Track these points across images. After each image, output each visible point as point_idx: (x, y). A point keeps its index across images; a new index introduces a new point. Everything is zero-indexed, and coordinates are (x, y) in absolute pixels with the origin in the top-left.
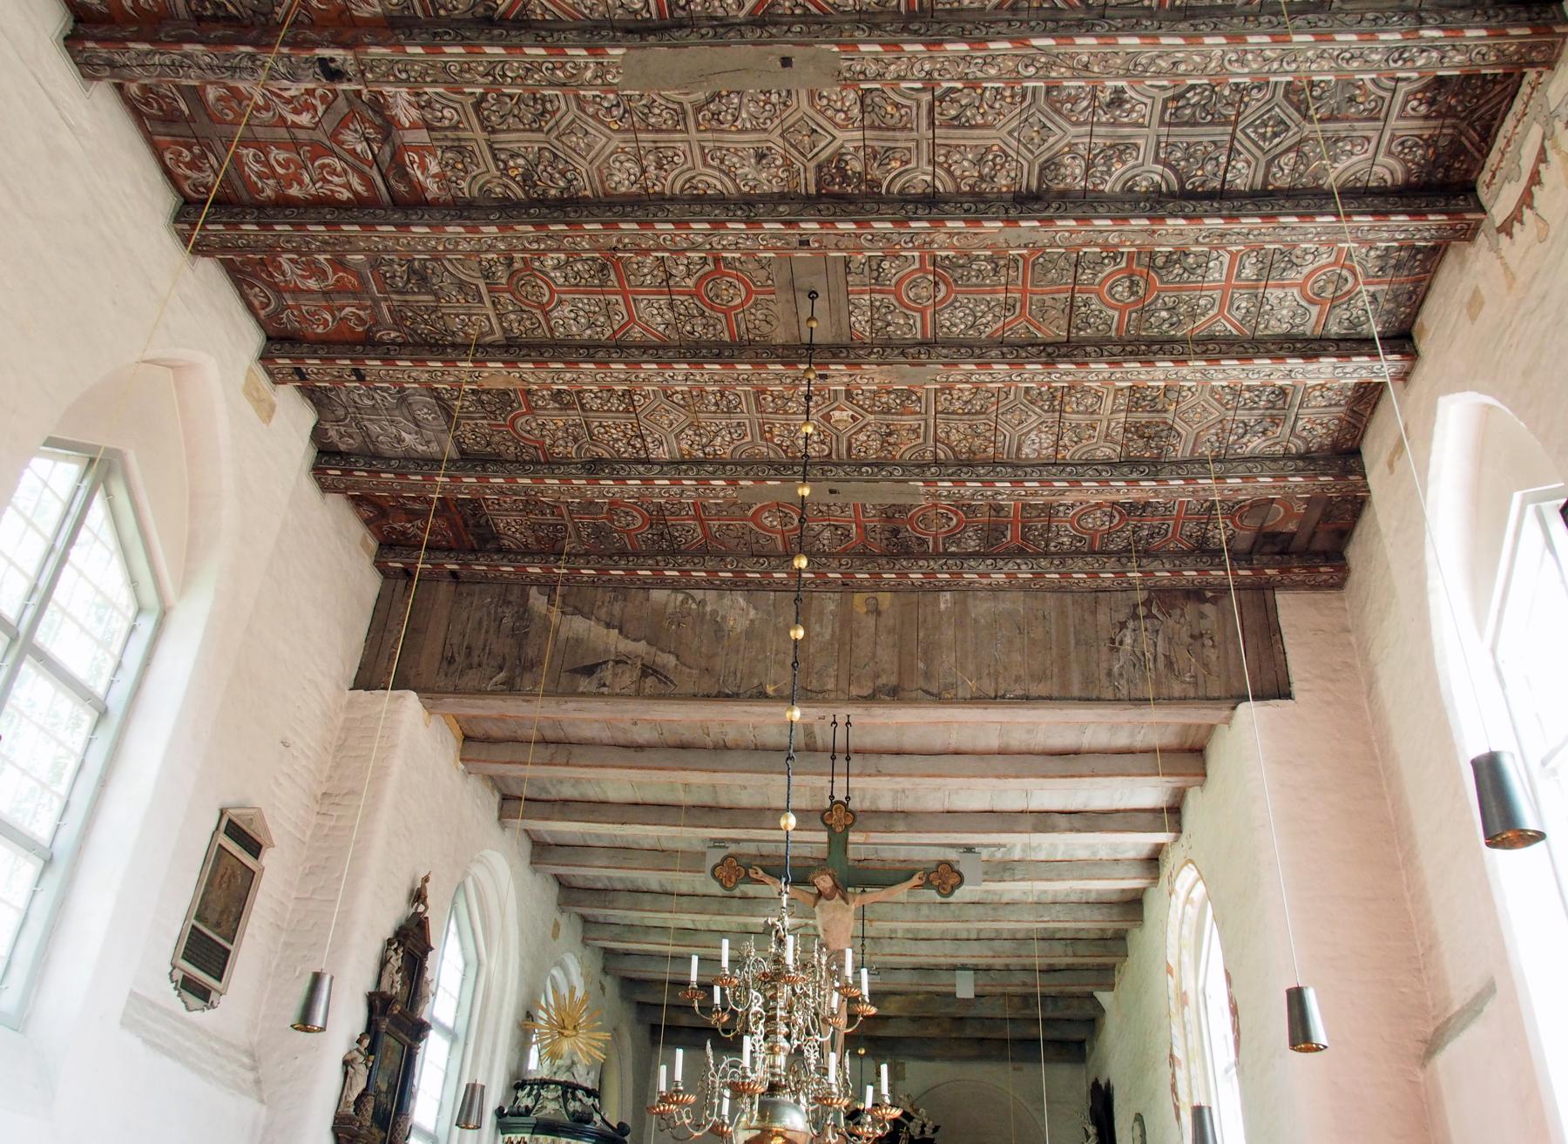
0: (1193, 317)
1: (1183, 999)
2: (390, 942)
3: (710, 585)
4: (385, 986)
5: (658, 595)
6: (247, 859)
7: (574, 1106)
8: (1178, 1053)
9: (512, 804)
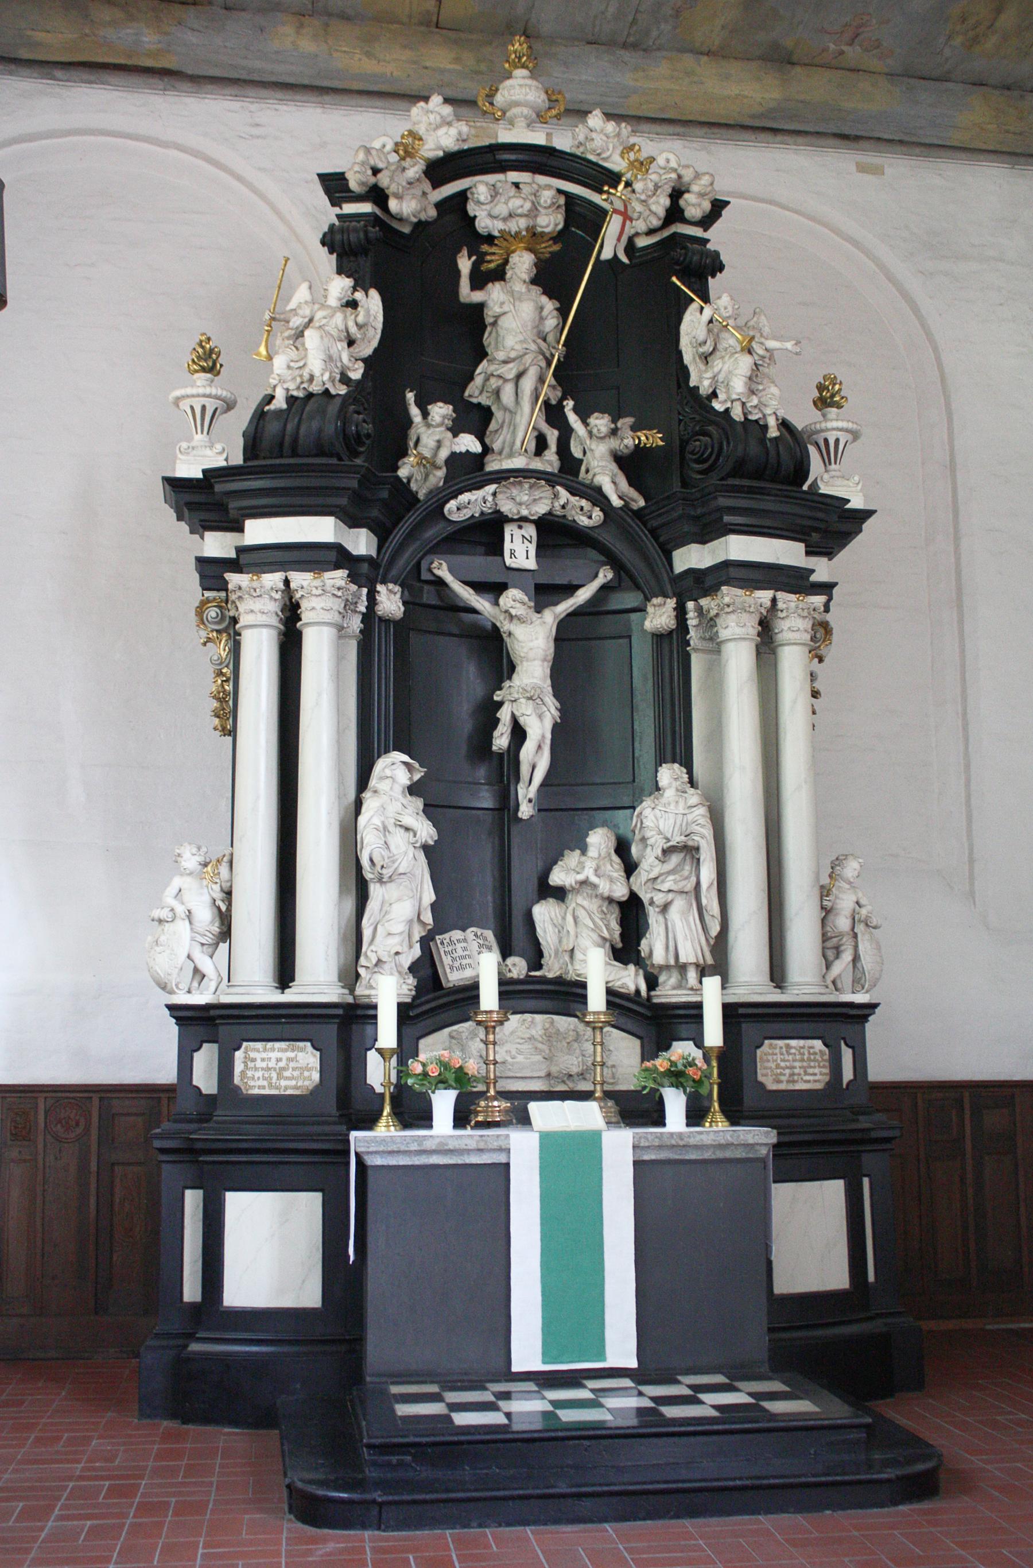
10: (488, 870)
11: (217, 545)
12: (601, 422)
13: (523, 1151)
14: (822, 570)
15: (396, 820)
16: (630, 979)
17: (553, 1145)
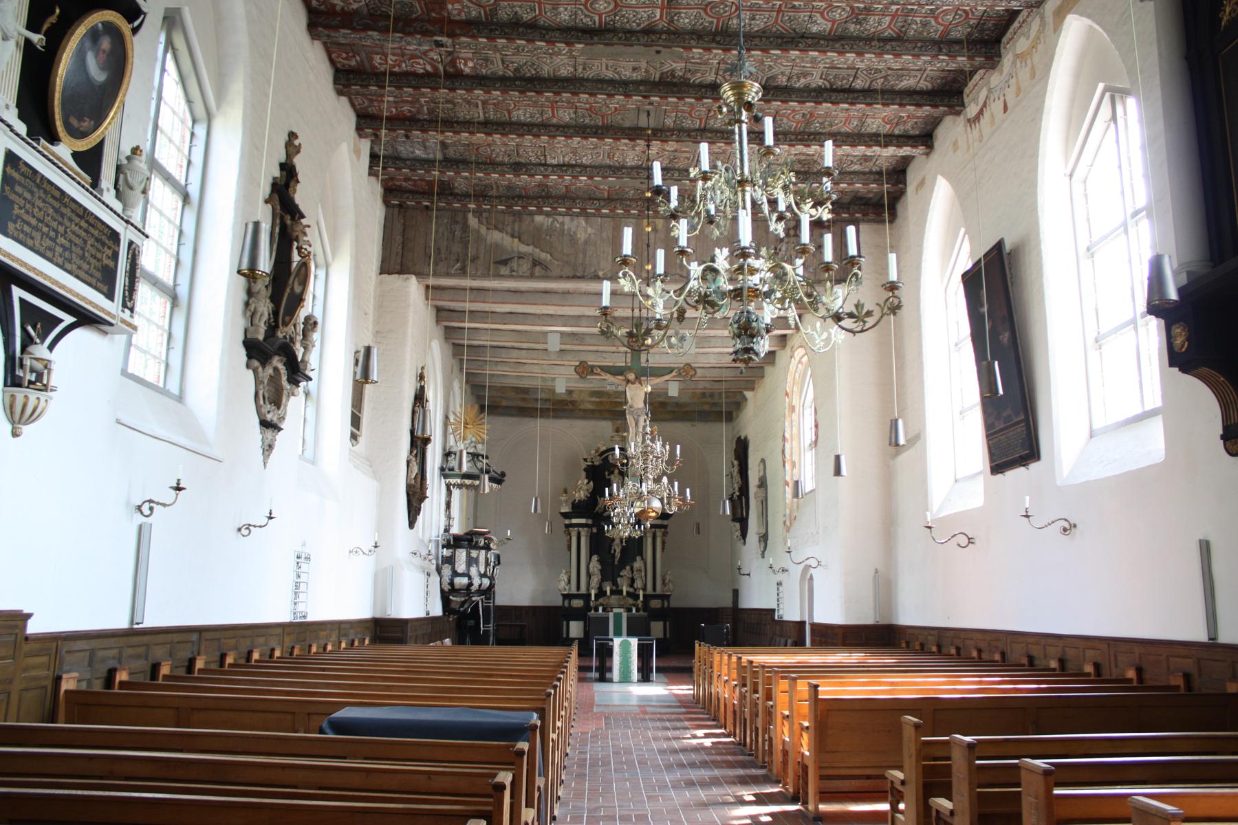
0: (831, 126)
1: (793, 409)
3: (566, 214)
5: (539, 219)
7: (479, 465)
8: (787, 435)
9: (444, 314)
10: (610, 572)
11: (567, 522)
13: (611, 615)
14: (665, 522)
15: (595, 566)
16: (631, 590)
17: (615, 614)
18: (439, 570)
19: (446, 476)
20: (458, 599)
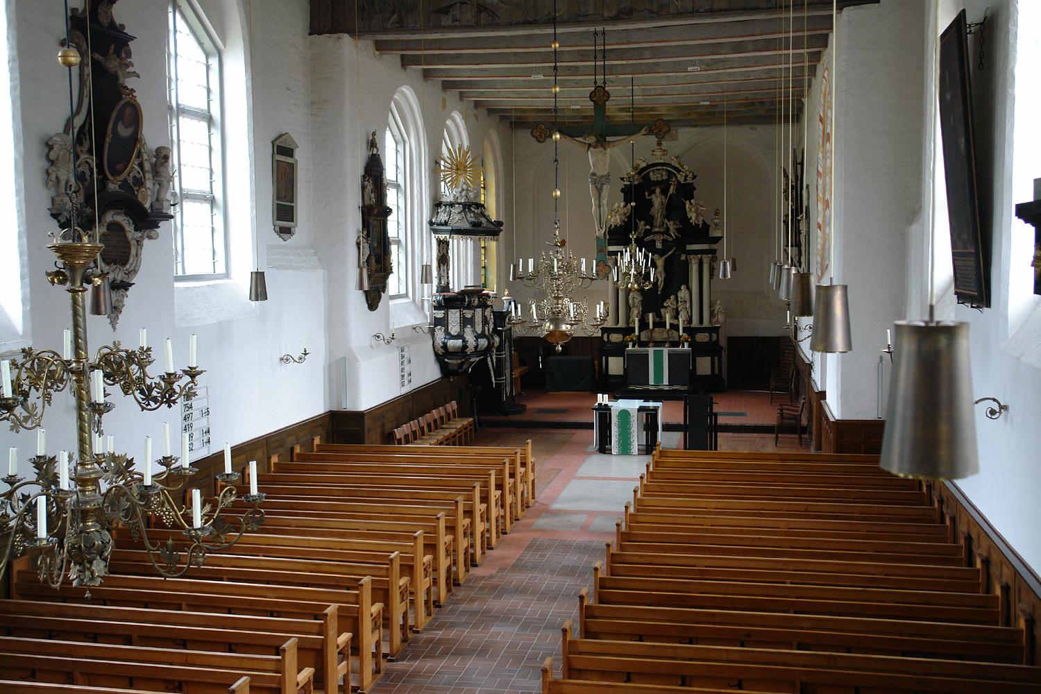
2: (364, 177)
4: (367, 202)
6: (289, 160)
12: (671, 223)
16: (675, 322)
18: (432, 332)
19: (436, 232)
20: (455, 362)
